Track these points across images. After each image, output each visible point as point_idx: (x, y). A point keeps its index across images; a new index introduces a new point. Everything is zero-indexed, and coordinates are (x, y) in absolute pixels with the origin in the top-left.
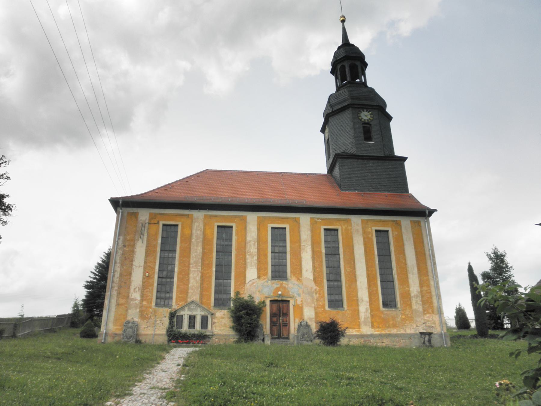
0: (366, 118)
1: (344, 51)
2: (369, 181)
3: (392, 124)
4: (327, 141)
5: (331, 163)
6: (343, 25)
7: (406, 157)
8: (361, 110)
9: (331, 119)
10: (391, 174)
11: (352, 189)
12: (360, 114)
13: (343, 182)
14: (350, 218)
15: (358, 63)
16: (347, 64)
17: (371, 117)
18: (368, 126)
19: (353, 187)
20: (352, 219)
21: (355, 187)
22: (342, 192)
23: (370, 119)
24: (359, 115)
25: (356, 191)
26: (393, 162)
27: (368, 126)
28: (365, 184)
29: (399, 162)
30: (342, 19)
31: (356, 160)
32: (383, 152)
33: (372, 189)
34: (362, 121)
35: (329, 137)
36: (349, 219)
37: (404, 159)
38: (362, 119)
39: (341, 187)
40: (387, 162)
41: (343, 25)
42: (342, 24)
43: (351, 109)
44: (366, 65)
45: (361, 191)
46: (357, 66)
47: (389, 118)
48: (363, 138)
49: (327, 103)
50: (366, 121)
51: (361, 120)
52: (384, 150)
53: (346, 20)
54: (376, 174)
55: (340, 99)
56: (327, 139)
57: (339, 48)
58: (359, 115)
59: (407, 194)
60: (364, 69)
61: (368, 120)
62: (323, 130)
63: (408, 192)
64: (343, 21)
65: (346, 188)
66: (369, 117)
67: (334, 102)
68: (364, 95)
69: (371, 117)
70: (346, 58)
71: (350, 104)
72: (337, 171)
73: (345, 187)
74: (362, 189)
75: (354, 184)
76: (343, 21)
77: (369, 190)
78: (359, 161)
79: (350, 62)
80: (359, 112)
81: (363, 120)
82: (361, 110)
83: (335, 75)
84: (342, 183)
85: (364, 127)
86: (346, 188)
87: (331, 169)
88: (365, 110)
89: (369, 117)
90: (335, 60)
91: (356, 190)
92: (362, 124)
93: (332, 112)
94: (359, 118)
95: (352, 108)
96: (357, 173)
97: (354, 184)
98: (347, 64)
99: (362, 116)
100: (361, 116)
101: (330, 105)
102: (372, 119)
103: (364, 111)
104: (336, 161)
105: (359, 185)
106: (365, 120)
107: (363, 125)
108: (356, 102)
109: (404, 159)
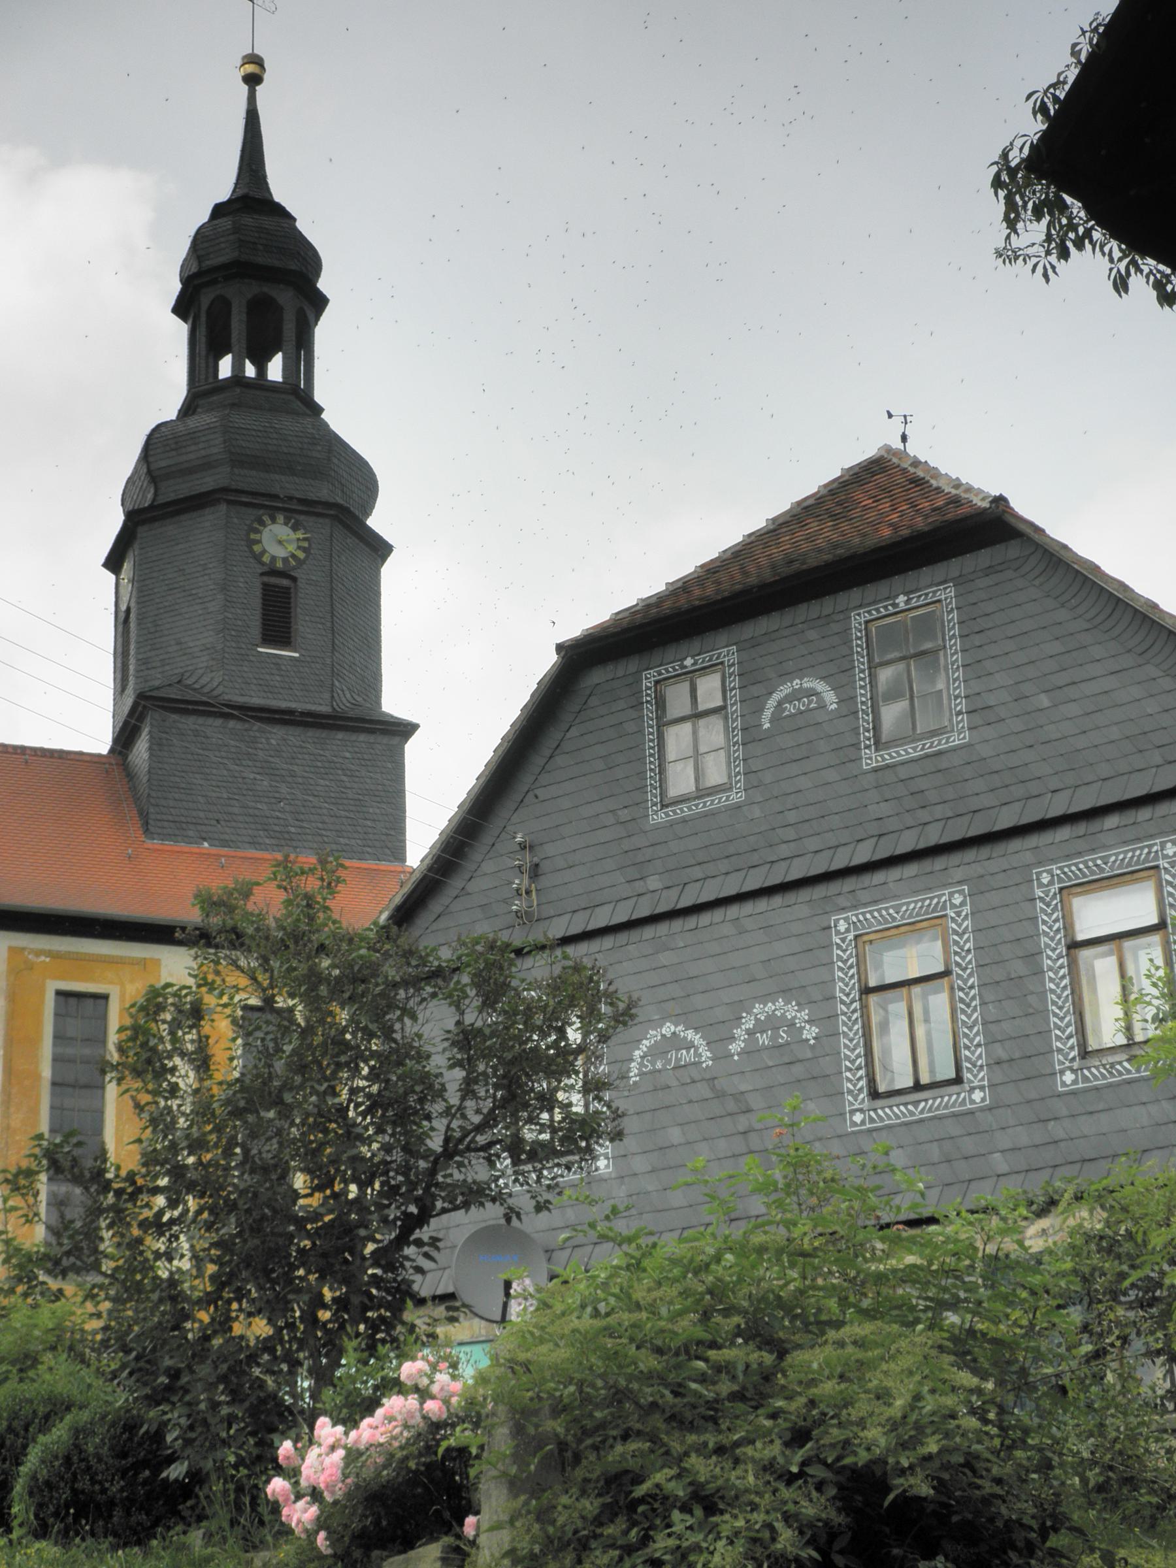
0: (280, 553)
1: (232, 237)
2: (259, 806)
3: (390, 574)
4: (122, 616)
5: (126, 709)
6: (252, 99)
7: (415, 720)
8: (265, 518)
9: (142, 531)
10: (348, 785)
11: (191, 833)
12: (258, 531)
13: (157, 805)
14: (156, 957)
15: (285, 297)
16: (239, 296)
17: (299, 548)
18: (285, 582)
19: (191, 827)
20: (164, 963)
21: (200, 828)
22: (149, 843)
23: (293, 556)
24: (253, 536)
25: (206, 844)
26: (362, 737)
27: (285, 582)
28: (241, 818)
29: (385, 740)
30: (250, 68)
31: (219, 722)
32: (327, 696)
33: (267, 841)
34: (263, 564)
35: (133, 605)
36: (152, 959)
37: (405, 730)
38: (264, 551)
39: (147, 823)
40: (340, 735)
41: (252, 99)
42: (245, 88)
43: (223, 507)
44: (319, 302)
45: (225, 843)
46: (279, 309)
47: (380, 549)
48: (256, 630)
49: (139, 461)
50: (279, 565)
51: (258, 558)
52: (333, 684)
53: (266, 77)
54: (290, 779)
55: (192, 456)
56: (123, 608)
57: (219, 211)
58: (253, 536)
59: (395, 866)
60: (311, 317)
61: (285, 560)
62: (113, 562)
63: (404, 860)
64: (253, 80)
65: (165, 831)
66: (292, 548)
67: (163, 464)
68: (286, 450)
69: (299, 548)
70: (239, 270)
71: (225, 490)
72: (141, 749)
73: (166, 824)
74: (227, 837)
75: (201, 814)
76: (253, 80)
77: (254, 844)
78: (232, 724)
79: (253, 289)
80: (256, 525)
81: (266, 559)
82: (265, 518)
83: (190, 321)
84: (152, 810)
85: (266, 587)
86: (165, 831)
87: (125, 737)
88: (280, 518)
89: (292, 548)
90: (194, 269)
91: (204, 839)
92: (262, 574)
93: (152, 507)
94: (252, 551)
95: (229, 502)
96: (214, 771)
97: (201, 814)
98: (239, 296)
99: (264, 541)
100: (259, 542)
101: (149, 472)
102: (301, 555)
103: (274, 520)
104: (141, 718)
105: (218, 821)
106: (274, 558)
107: (266, 579)
108: (251, 479)
109: (405, 730)
